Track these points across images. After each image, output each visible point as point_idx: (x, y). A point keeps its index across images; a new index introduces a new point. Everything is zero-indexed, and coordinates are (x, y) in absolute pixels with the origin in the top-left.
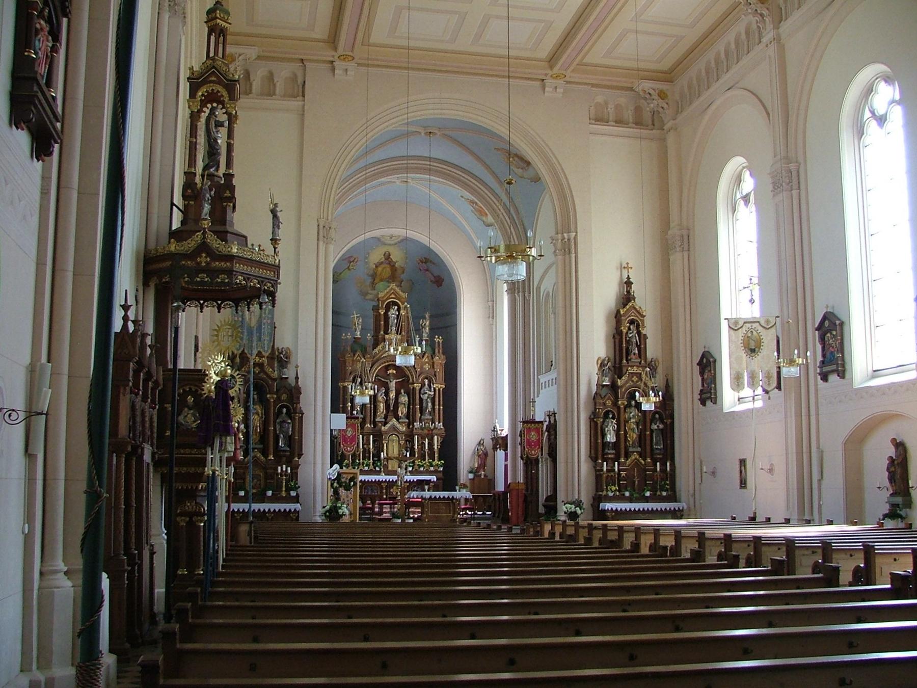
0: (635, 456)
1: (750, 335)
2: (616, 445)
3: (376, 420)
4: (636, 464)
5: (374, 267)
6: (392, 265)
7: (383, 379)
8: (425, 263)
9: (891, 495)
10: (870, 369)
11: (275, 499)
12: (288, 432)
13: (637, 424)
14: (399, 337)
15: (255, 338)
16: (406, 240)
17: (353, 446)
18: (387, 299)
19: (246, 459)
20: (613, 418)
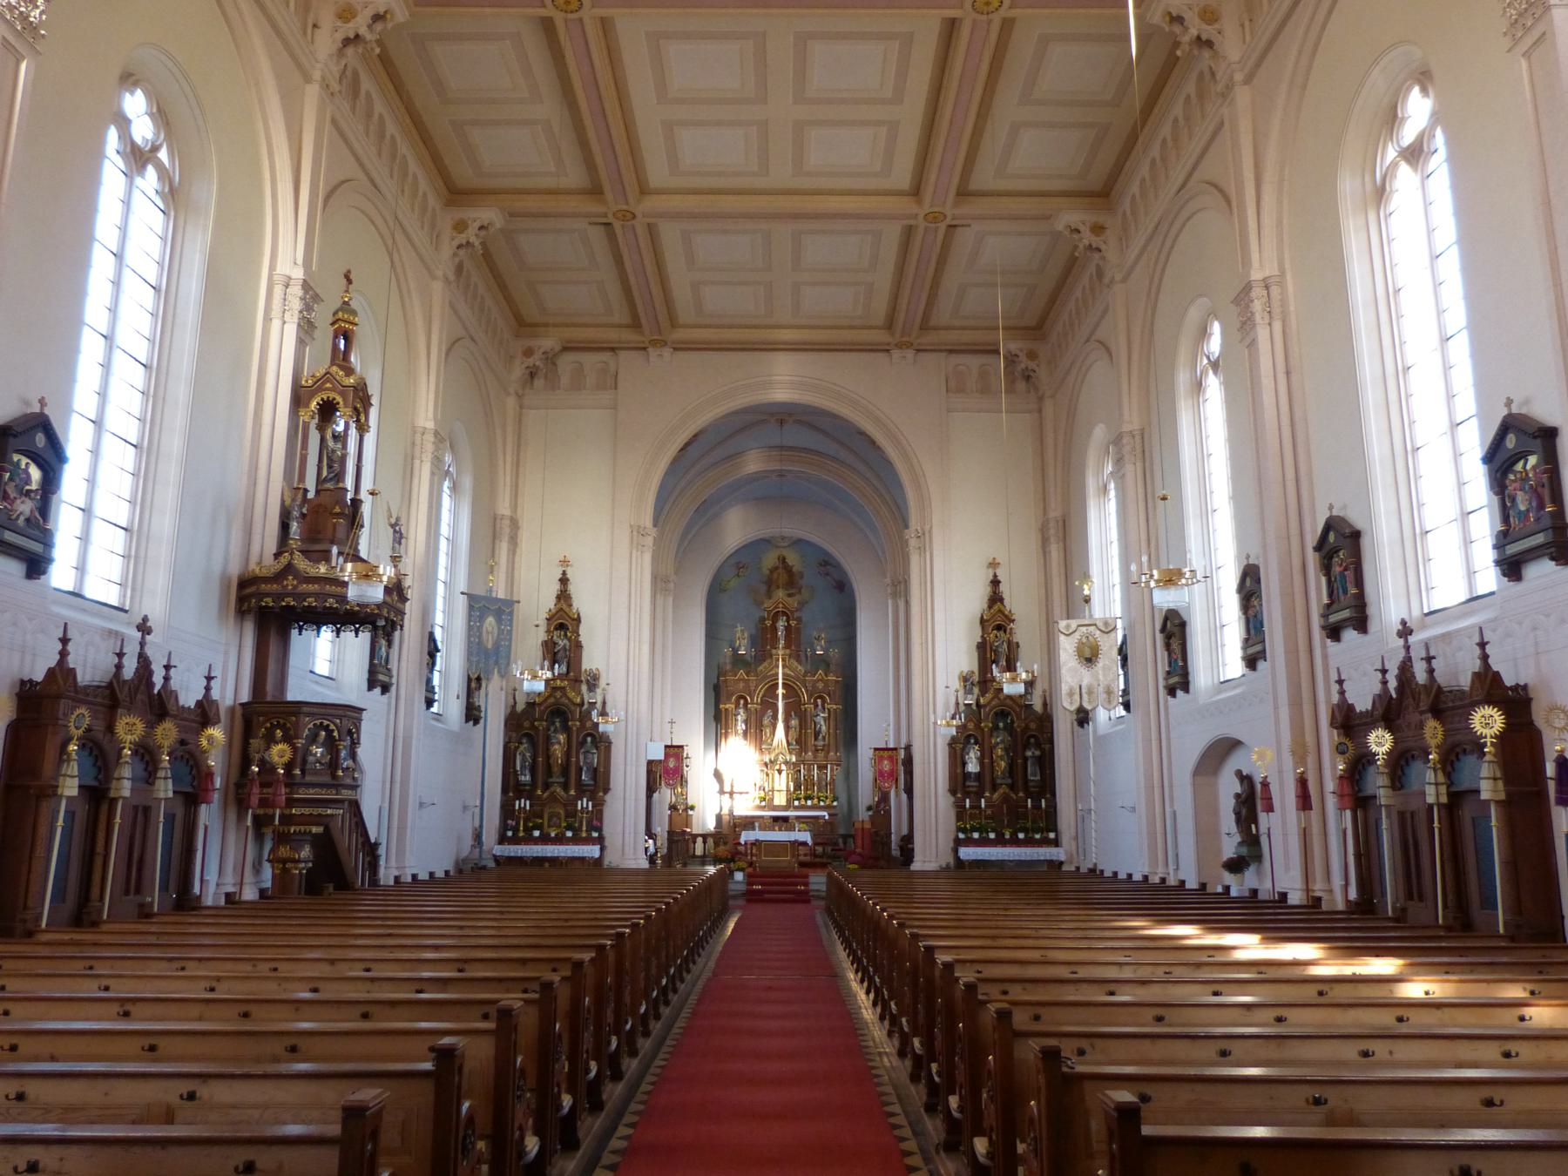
0: (1002, 790)
1: (1084, 640)
2: (979, 776)
4: (1005, 798)
5: (768, 572)
6: (788, 569)
9: (1240, 844)
10: (1216, 681)
11: (576, 840)
12: (593, 764)
13: (1006, 750)
14: (788, 651)
15: (491, 662)
16: (798, 543)
19: (545, 795)
20: (976, 743)
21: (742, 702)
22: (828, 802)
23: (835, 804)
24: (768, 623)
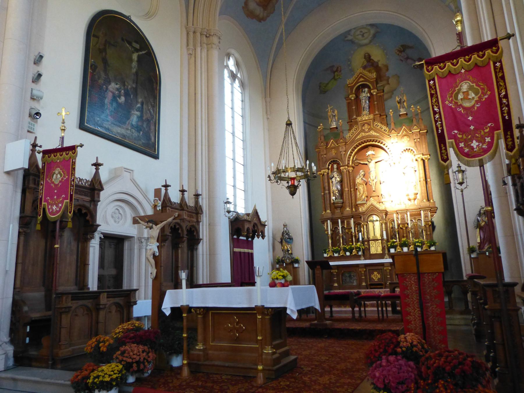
3: (357, 203)
7: (362, 162)
8: (404, 51)
17: (62, 202)
18: (355, 84)
21: (335, 166)
22: (425, 247)
23: (433, 248)
24: (352, 97)
